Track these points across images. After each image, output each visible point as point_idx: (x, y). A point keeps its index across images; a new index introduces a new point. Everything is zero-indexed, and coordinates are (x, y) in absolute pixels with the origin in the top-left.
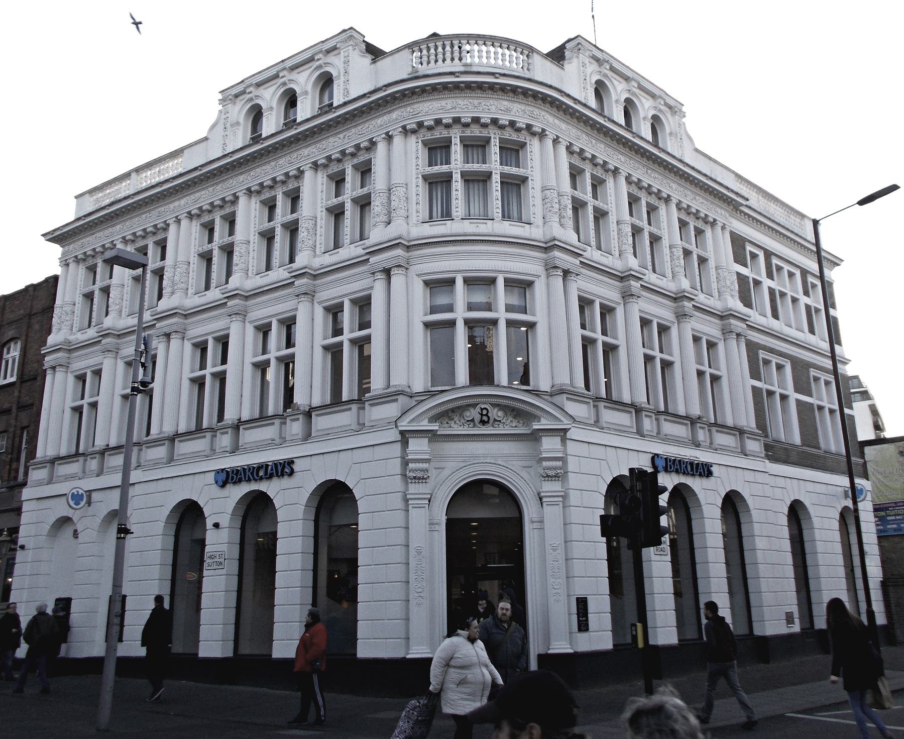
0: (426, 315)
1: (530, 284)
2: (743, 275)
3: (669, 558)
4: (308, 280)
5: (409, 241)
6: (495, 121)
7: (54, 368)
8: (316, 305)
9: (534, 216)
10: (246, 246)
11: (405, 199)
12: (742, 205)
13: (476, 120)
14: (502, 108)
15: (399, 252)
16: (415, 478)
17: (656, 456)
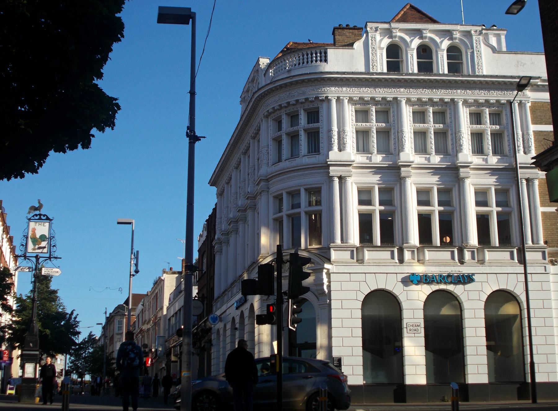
0: (274, 214)
1: (320, 188)
2: (547, 131)
3: (423, 334)
4: (251, 201)
5: (266, 177)
6: (297, 101)
7: (216, 253)
8: (256, 212)
9: (322, 149)
10: (244, 182)
11: (266, 154)
12: (538, 82)
13: (288, 103)
14: (301, 92)
15: (262, 184)
16: (264, 300)
17: (411, 276)
